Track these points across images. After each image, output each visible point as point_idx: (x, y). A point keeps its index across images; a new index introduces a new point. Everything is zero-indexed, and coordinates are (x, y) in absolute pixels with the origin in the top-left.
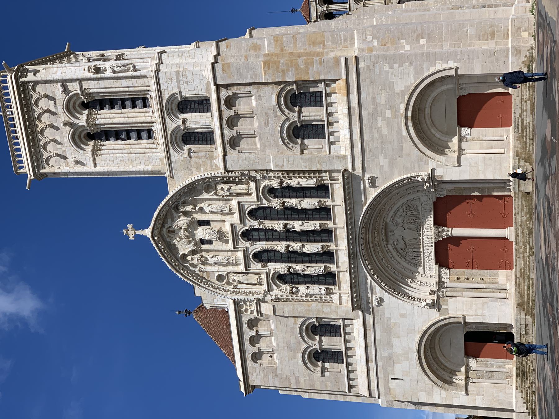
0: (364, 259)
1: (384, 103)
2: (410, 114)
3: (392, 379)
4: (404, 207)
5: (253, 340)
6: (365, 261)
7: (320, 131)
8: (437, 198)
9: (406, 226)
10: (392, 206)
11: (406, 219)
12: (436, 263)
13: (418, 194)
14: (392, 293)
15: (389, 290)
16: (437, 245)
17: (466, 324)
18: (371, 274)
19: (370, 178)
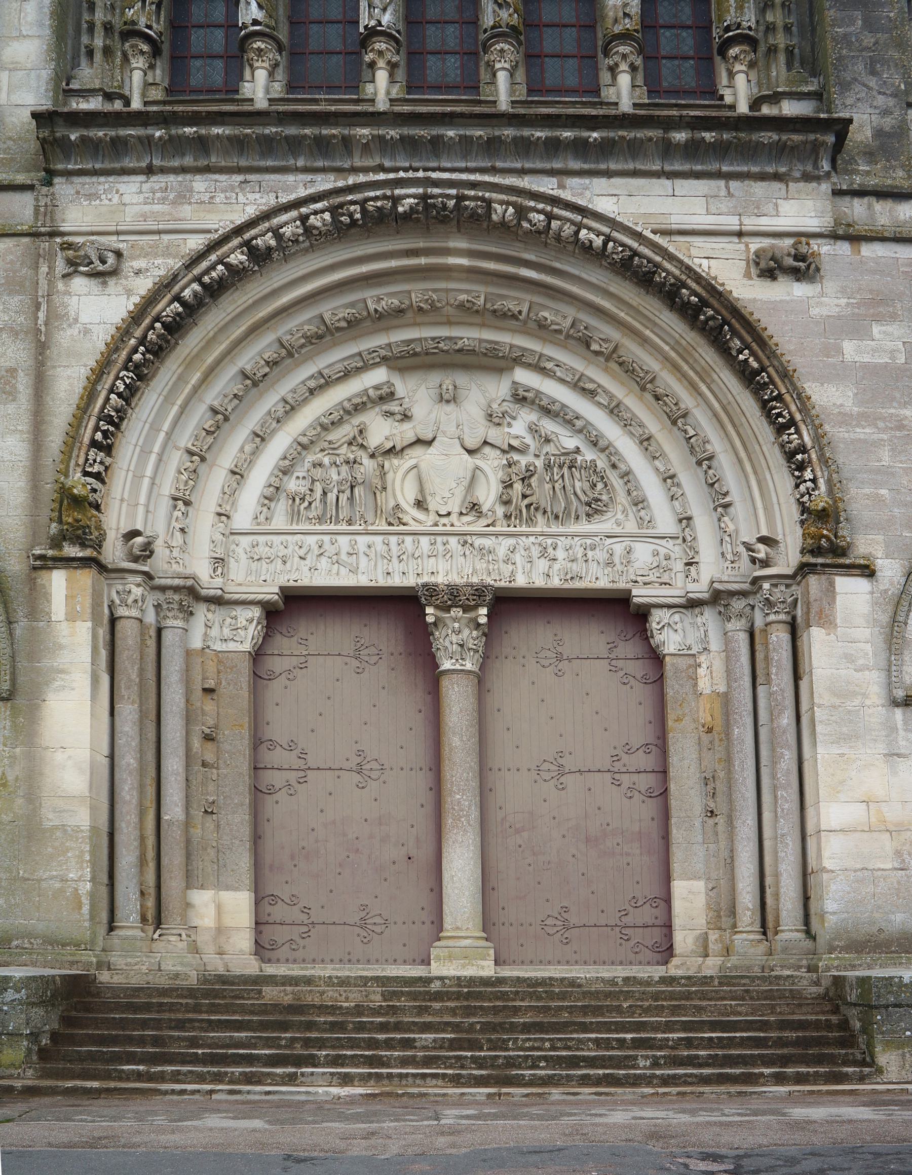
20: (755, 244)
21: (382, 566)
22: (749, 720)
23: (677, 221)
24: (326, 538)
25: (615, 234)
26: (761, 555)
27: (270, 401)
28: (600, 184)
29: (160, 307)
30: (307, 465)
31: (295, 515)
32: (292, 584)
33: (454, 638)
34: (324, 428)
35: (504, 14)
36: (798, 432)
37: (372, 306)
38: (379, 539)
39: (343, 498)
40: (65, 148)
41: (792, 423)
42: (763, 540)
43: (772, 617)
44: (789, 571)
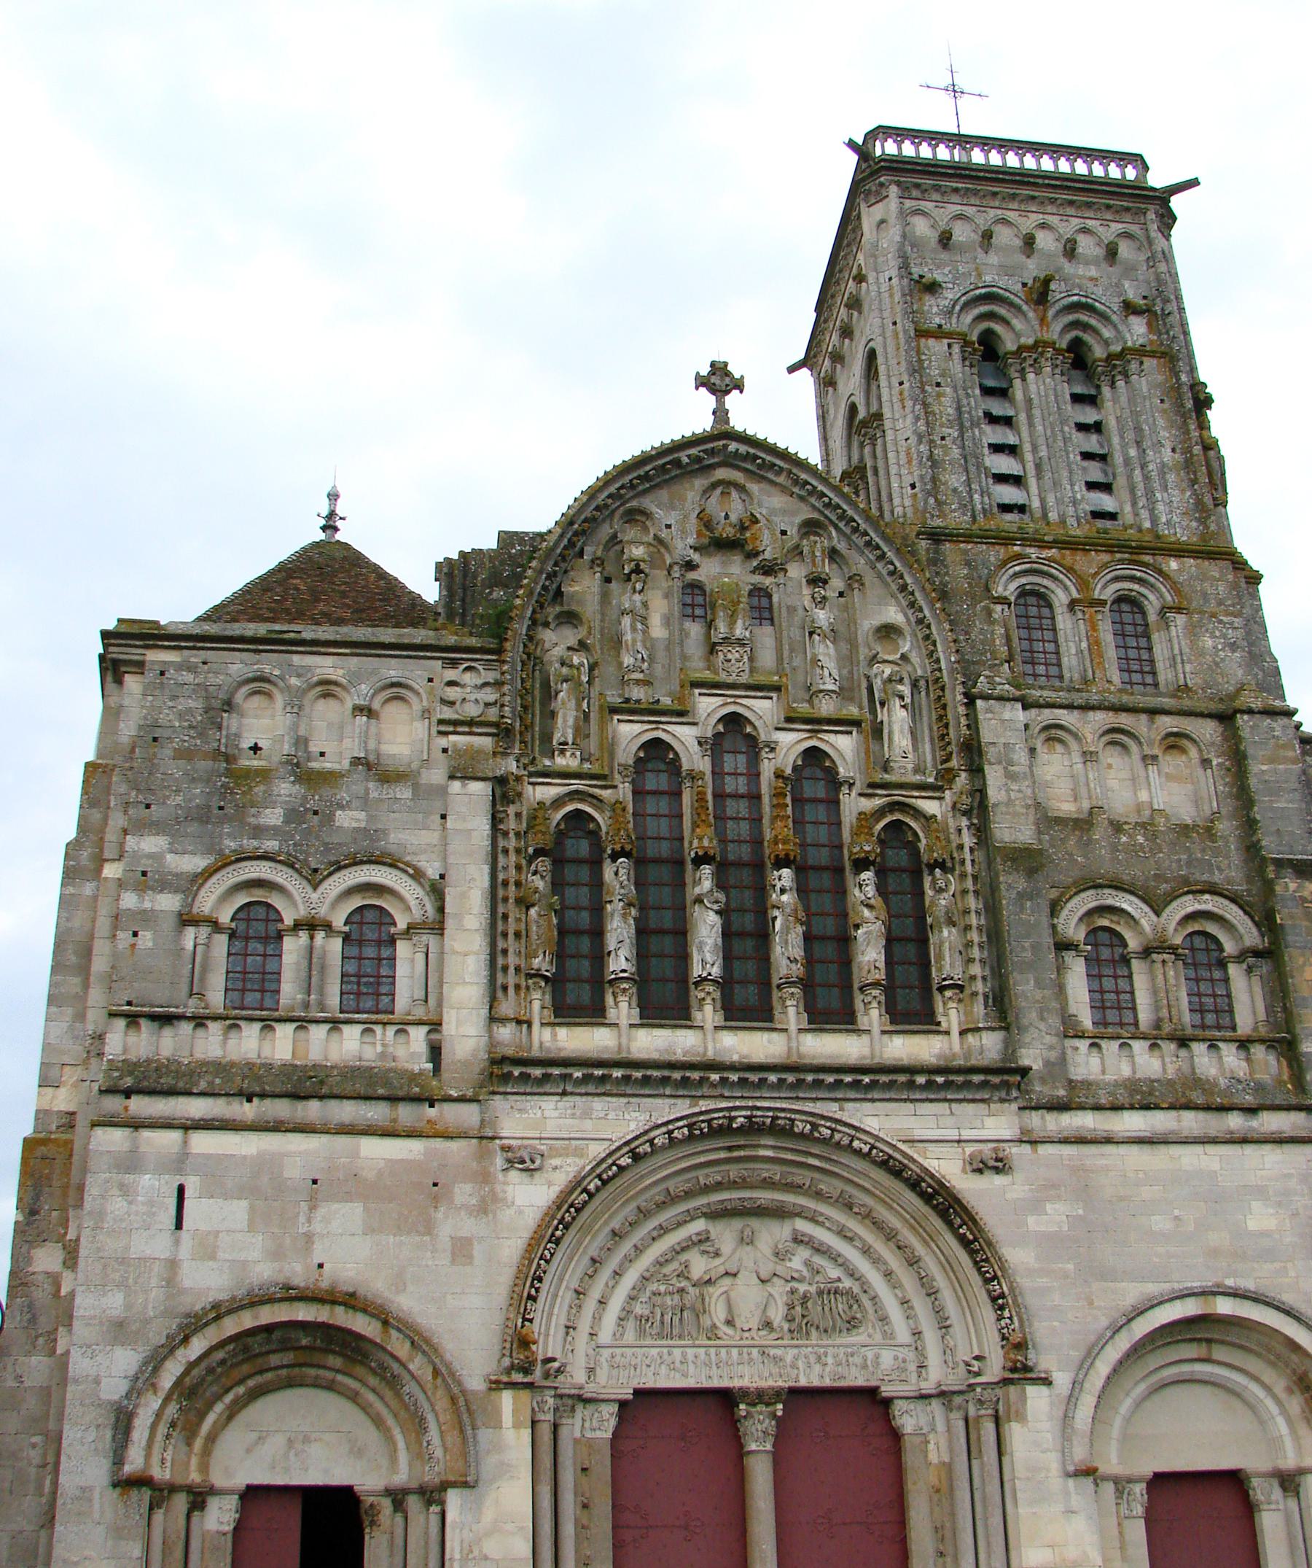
0: (695, 1123)
1: (1252, 1225)
2: (1224, 1306)
3: (181, 1190)
4: (847, 1283)
5: (326, 695)
6: (690, 1126)
7: (1112, 1016)
8: (887, 1402)
9: (779, 1290)
10: (857, 1243)
11: (802, 1288)
12: (637, 1392)
13: (903, 1335)
14: (559, 1216)
15: (571, 1206)
16: (725, 1398)
17: (433, 1495)
18: (637, 1143)
19: (1000, 1164)
20: (969, 1149)
21: (705, 1371)
22: (967, 1485)
23: (919, 1133)
24: (665, 1350)
25: (878, 1144)
26: (976, 1369)
27: (626, 1247)
28: (867, 1106)
29: (574, 1196)
30: (648, 1294)
31: (641, 1332)
32: (641, 1386)
33: (759, 1427)
34: (661, 1264)
35: (793, 966)
36: (999, 1283)
37: (702, 1181)
38: (702, 1350)
39: (676, 1319)
40: (506, 1078)
41: (995, 1277)
42: (977, 1358)
43: (983, 1412)
44: (996, 1380)
